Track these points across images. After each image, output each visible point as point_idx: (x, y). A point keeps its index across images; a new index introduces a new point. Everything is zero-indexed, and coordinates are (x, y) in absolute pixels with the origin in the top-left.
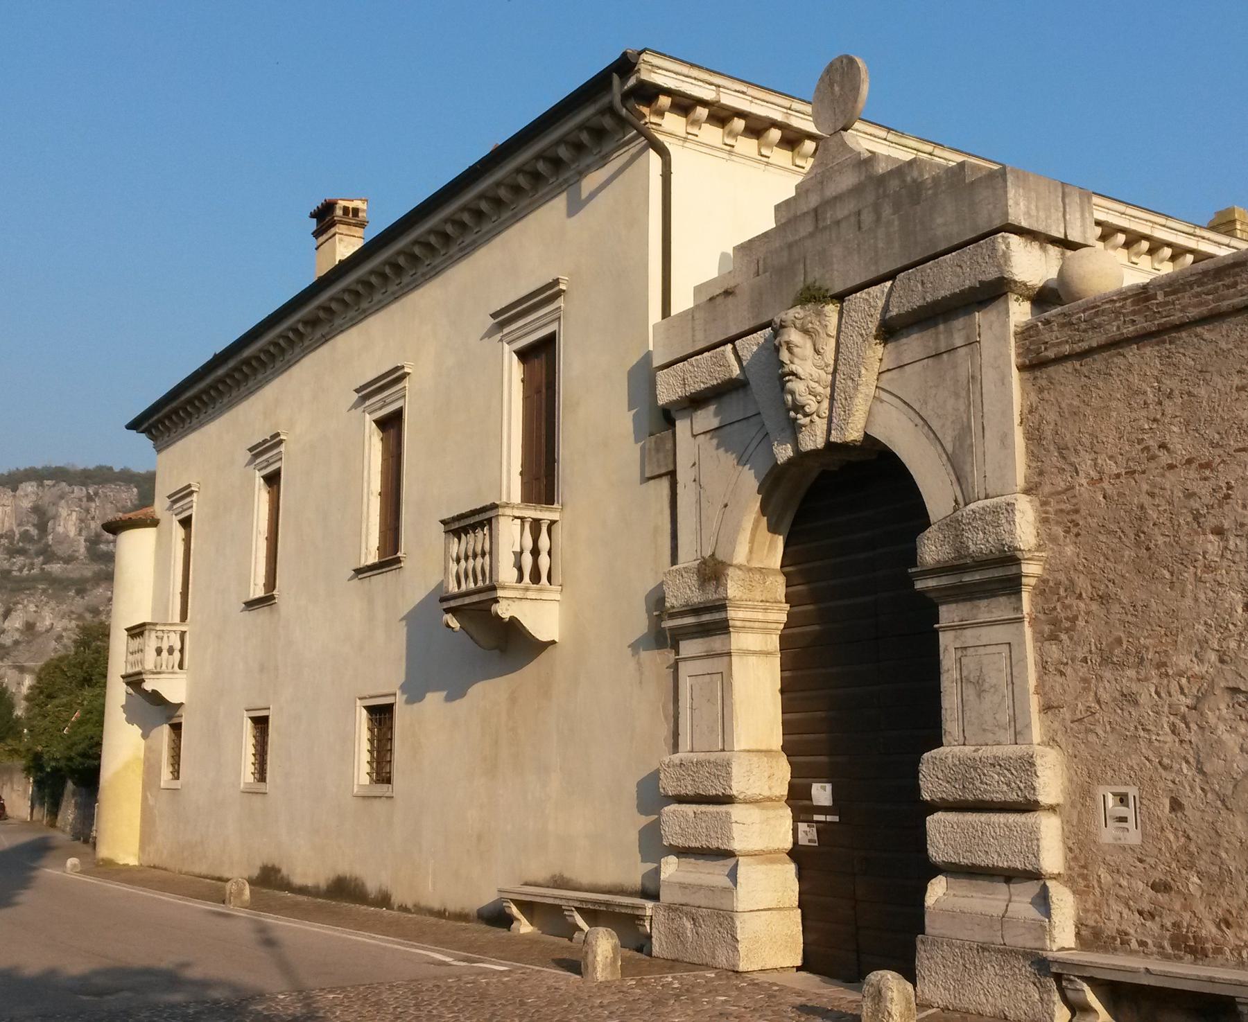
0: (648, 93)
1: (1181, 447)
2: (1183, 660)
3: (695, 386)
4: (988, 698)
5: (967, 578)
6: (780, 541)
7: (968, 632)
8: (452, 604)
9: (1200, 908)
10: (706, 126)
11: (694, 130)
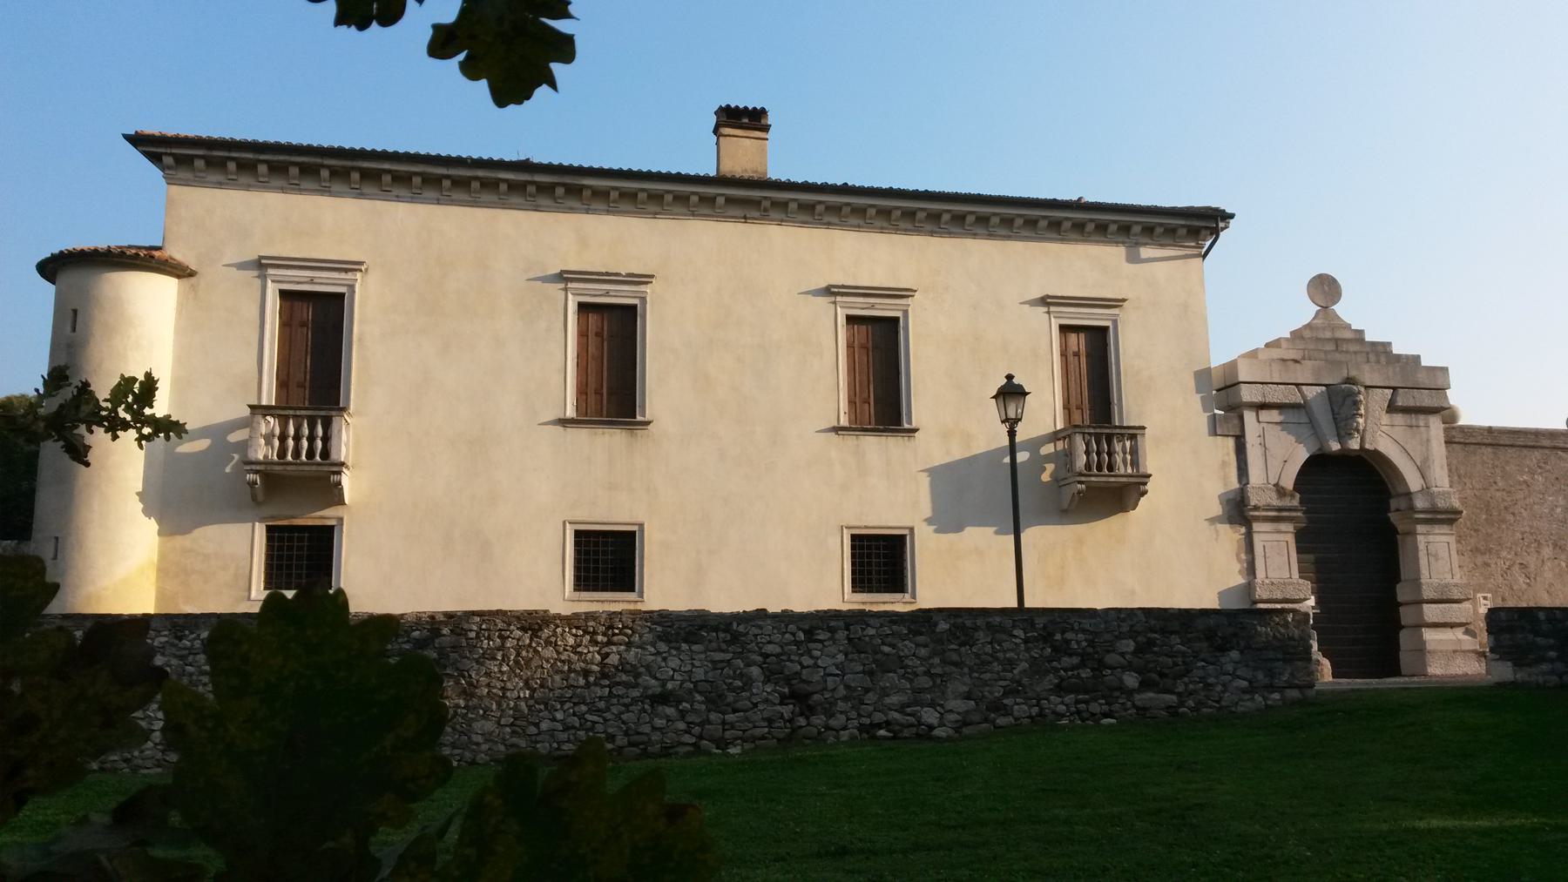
3: (1270, 399)
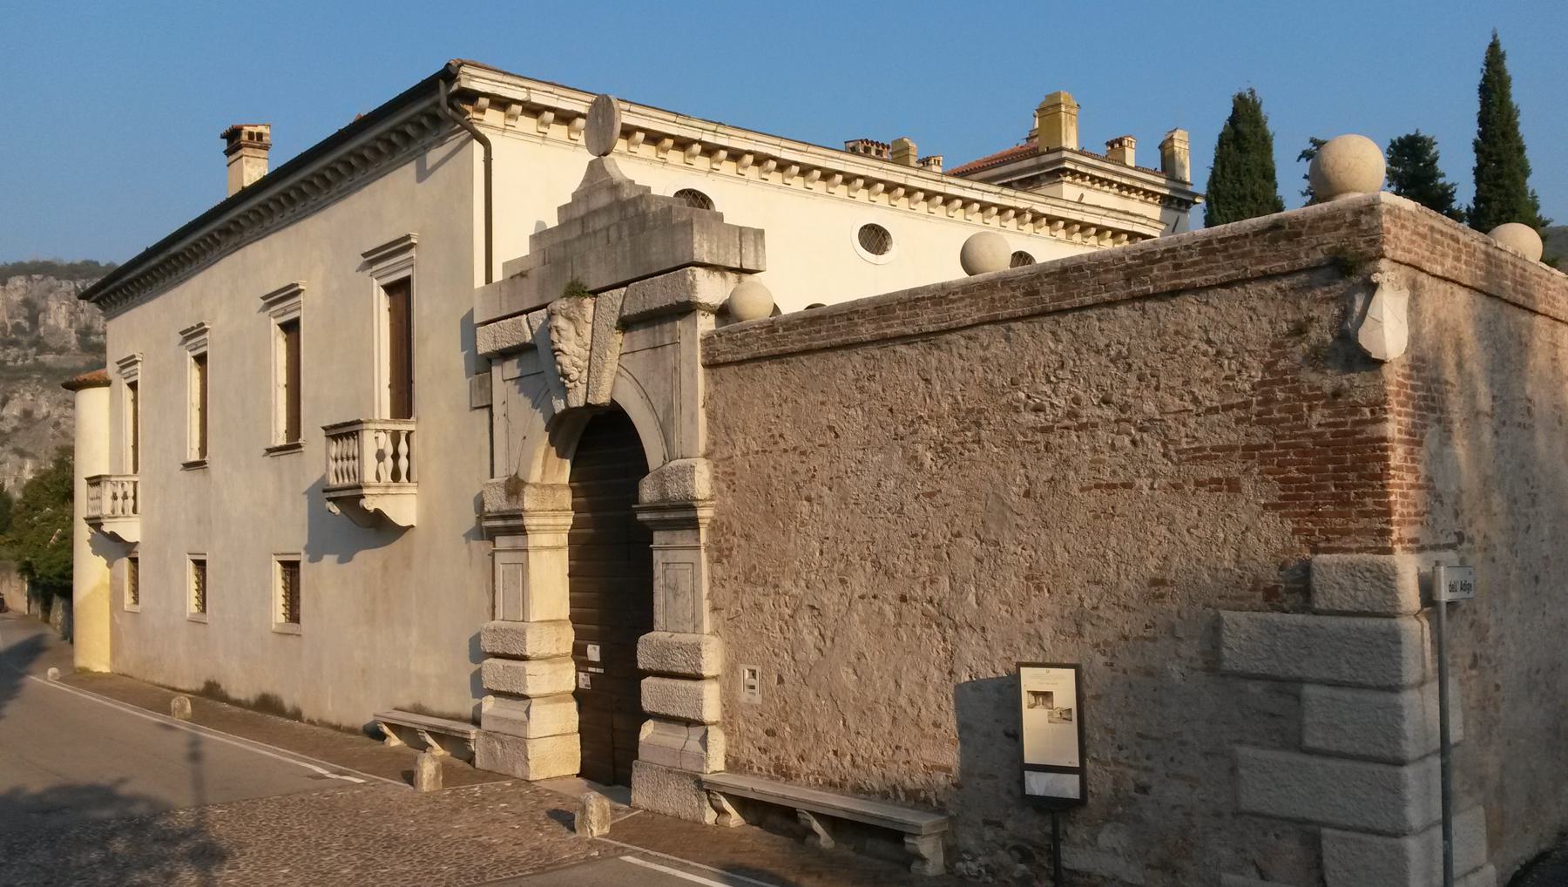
0: (472, 96)
1: (792, 439)
2: (787, 584)
3: (504, 344)
4: (681, 600)
5: (667, 516)
6: (567, 464)
7: (670, 553)
8: (332, 495)
9: (790, 748)
10: (522, 118)
11: (512, 122)
